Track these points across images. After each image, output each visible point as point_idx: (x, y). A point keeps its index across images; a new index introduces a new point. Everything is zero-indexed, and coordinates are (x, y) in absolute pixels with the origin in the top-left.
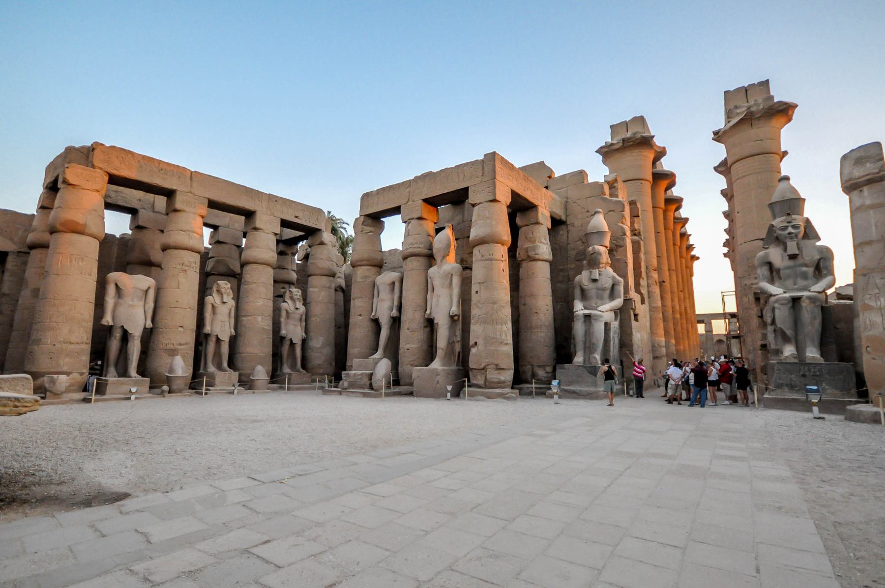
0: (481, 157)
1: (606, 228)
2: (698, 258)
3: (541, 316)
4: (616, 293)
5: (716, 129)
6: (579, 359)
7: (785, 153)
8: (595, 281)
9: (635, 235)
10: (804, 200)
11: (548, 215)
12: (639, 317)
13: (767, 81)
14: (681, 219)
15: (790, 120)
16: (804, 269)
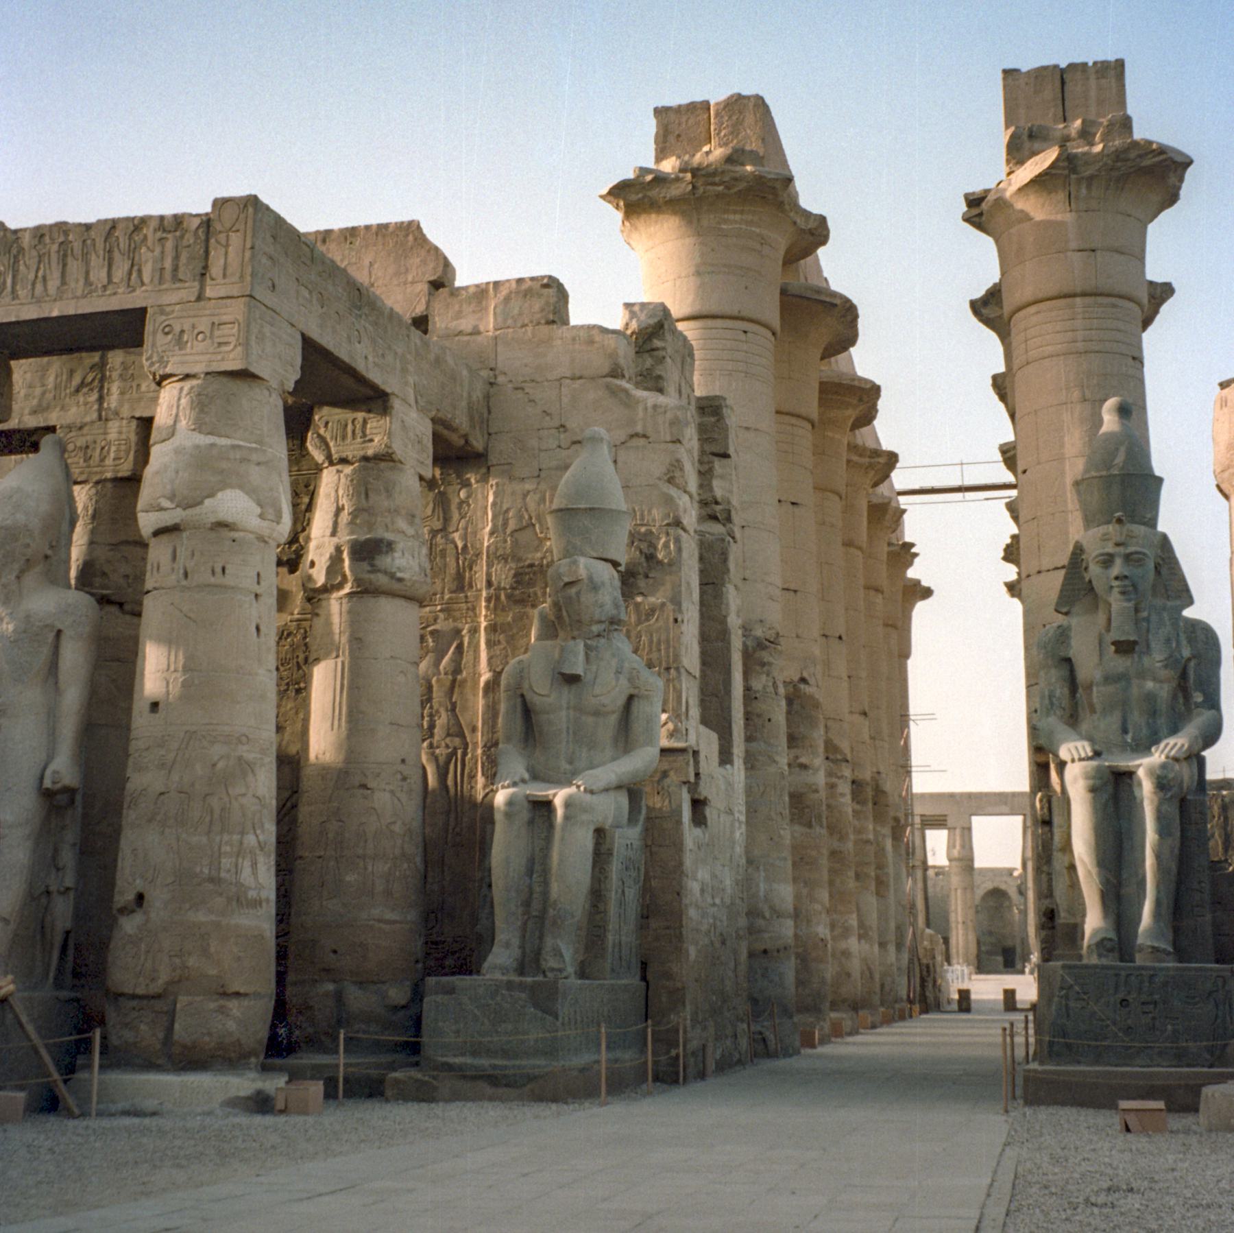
0: (204, 207)
1: (618, 500)
2: (927, 593)
3: (382, 799)
4: (638, 727)
5: (976, 187)
6: (501, 957)
7: (1162, 292)
8: (572, 680)
9: (713, 518)
10: (1160, 481)
11: (425, 429)
12: (709, 812)
13: (1120, 64)
14: (877, 452)
15: (1171, 198)
16: (1150, 685)
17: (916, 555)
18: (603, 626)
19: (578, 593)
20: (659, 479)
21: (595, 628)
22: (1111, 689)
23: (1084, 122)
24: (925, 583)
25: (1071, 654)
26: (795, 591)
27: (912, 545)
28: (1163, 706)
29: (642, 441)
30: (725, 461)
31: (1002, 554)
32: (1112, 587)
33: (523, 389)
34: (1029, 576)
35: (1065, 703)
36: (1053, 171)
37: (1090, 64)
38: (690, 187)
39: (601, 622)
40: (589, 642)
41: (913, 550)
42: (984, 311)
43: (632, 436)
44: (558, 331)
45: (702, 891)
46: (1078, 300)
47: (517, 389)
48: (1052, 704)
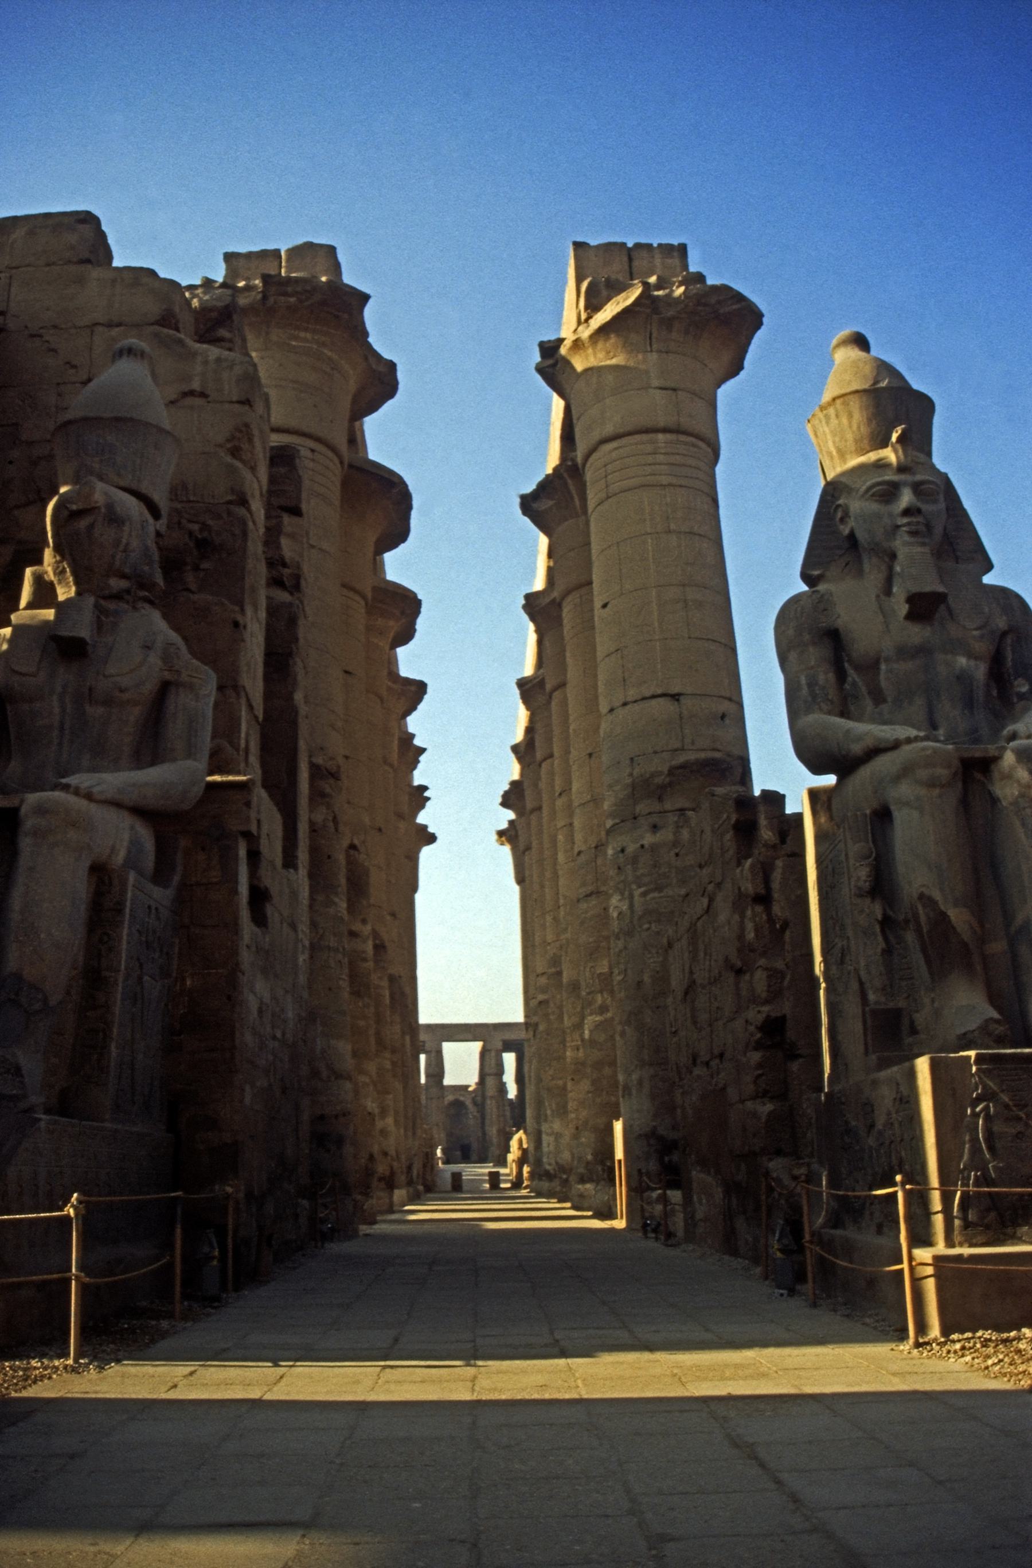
2: (431, 839)
16: (962, 661)
17: (428, 799)
18: (124, 584)
19: (91, 527)
20: (220, 446)
21: (116, 584)
22: (909, 666)
23: (659, 278)
24: (431, 830)
25: (839, 623)
27: (424, 788)
28: (980, 694)
29: (198, 401)
30: (295, 520)
31: (500, 800)
32: (898, 527)
33: (41, 336)
34: (611, 710)
35: (832, 693)
36: (637, 309)
37: (655, 245)
38: (260, 296)
39: (124, 576)
40: (102, 602)
41: (427, 794)
42: (535, 506)
43: (186, 394)
44: (95, 273)
45: (260, 1011)
46: (661, 436)
47: (32, 336)
48: (814, 696)
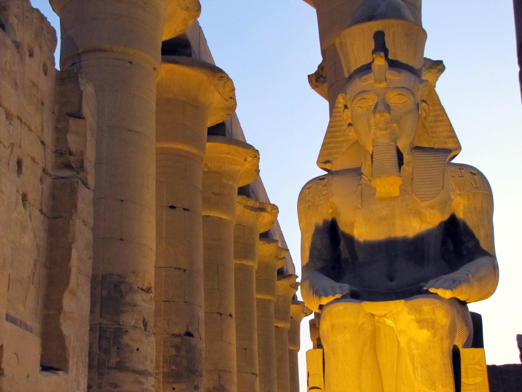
9: (68, 166)
26: (185, 270)
